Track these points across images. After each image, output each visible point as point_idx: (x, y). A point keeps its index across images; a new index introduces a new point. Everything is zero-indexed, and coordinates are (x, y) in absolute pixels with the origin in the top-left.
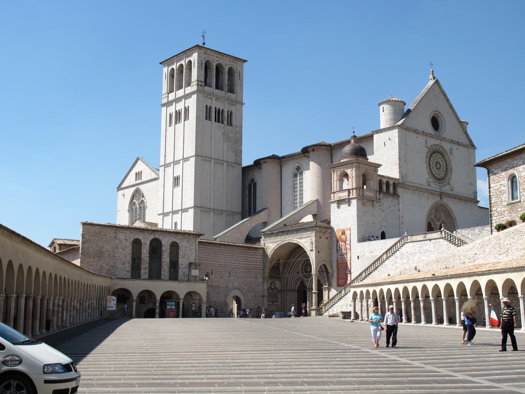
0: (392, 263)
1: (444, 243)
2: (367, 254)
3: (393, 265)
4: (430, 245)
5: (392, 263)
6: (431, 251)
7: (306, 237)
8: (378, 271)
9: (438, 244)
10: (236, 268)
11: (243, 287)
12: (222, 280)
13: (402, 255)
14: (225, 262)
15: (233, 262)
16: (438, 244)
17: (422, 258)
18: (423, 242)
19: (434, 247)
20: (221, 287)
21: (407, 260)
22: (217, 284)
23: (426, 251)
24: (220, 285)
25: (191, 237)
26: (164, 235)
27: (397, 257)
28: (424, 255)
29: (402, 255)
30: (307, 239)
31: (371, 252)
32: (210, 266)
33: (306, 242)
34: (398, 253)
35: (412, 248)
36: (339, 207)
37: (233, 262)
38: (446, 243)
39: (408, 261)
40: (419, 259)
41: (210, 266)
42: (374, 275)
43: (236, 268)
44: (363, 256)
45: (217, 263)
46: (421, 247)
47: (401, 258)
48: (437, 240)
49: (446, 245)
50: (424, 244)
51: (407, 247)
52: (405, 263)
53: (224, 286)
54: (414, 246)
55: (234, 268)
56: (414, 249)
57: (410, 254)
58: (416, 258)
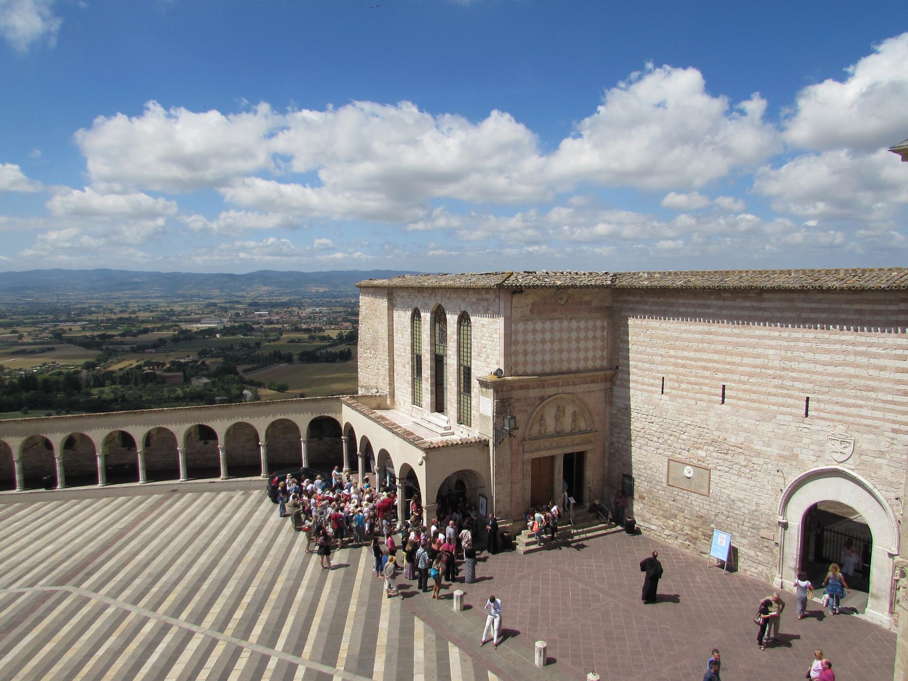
10: (843, 385)
11: (886, 472)
12: (766, 428)
14: (783, 359)
15: (826, 358)
20: (758, 454)
22: (741, 439)
24: (758, 446)
25: (491, 296)
26: (448, 295)
32: (717, 370)
37: (826, 358)
41: (717, 370)
43: (843, 385)
45: (746, 360)
53: (774, 450)
55: (834, 385)
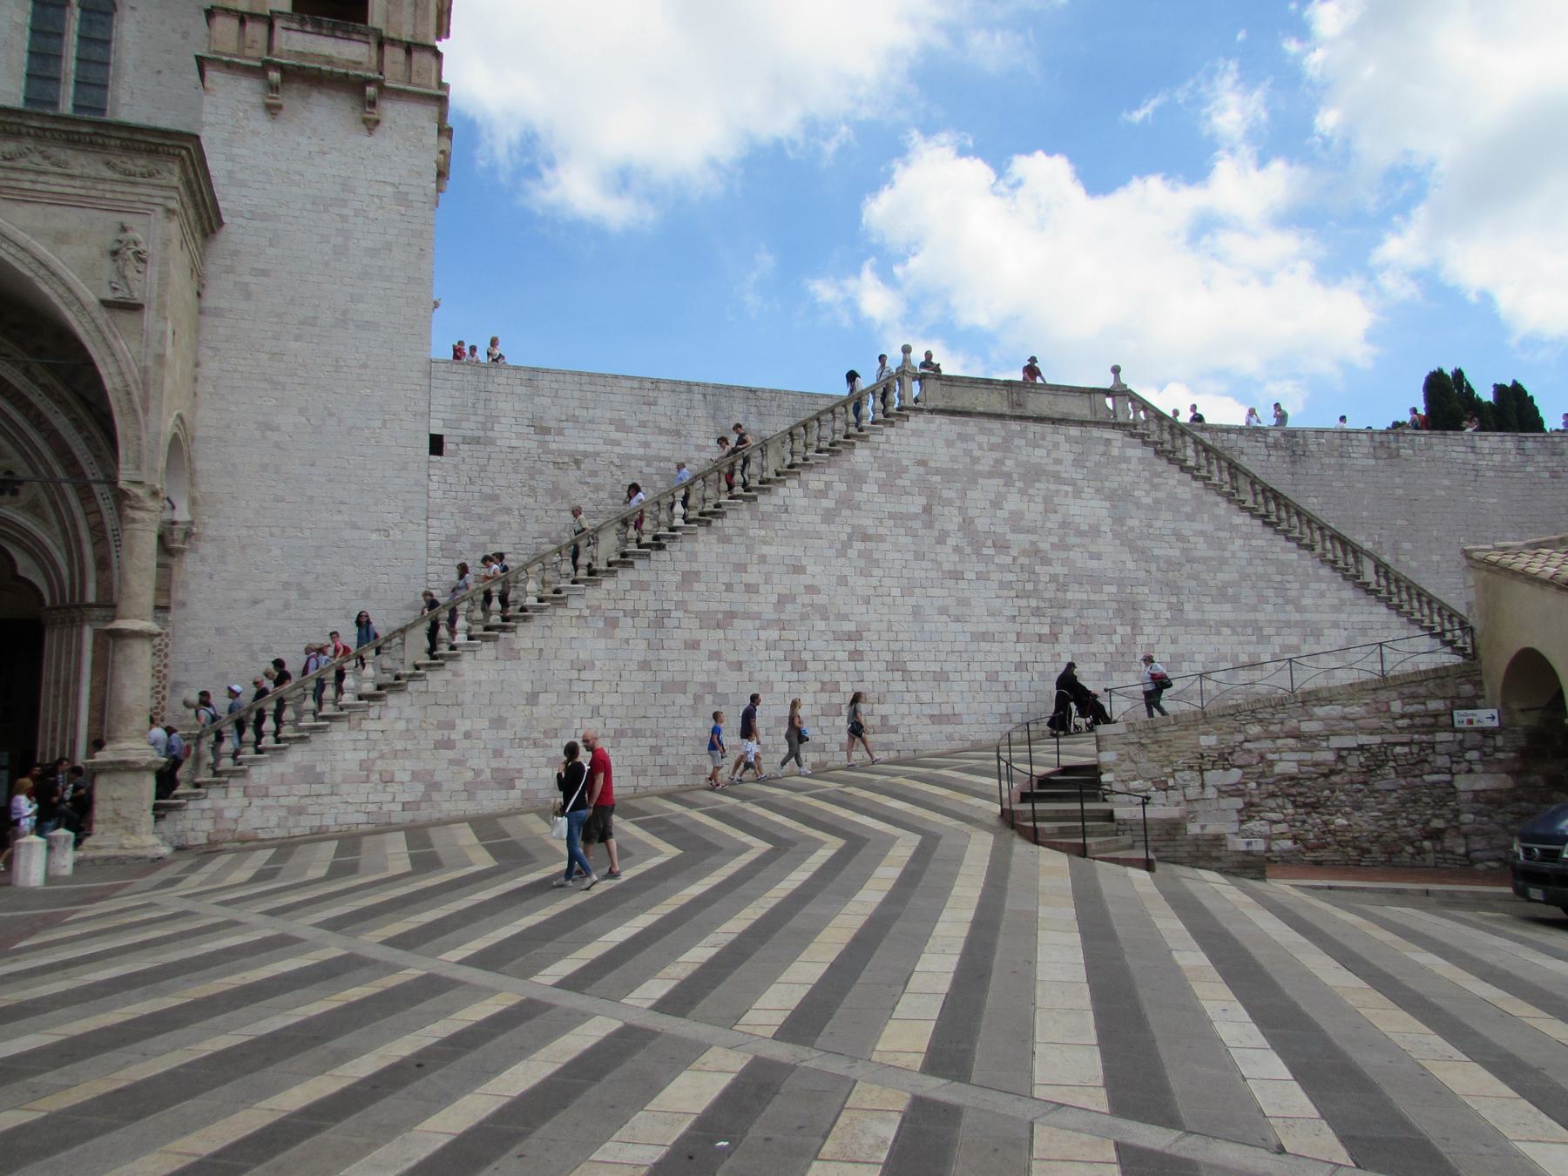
0: (828, 503)
1: (1130, 452)
2: (510, 434)
3: (829, 517)
4: (1056, 445)
5: (828, 503)
6: (1057, 478)
7: (60, 200)
8: (725, 539)
9: (1101, 449)
13: (894, 471)
16: (1101, 449)
17: (1013, 502)
18: (1015, 426)
19: (1078, 462)
21: (923, 500)
23: (1033, 474)
27: (857, 479)
28: (1022, 492)
29: (894, 471)
30: (70, 219)
31: (545, 431)
33: (61, 238)
34: (861, 455)
35: (949, 444)
36: (272, 109)
38: (1136, 452)
39: (927, 509)
40: (996, 504)
42: (693, 557)
44: (466, 441)
46: (1005, 446)
47: (886, 487)
48: (1096, 432)
49: (1141, 460)
50: (1023, 432)
51: (917, 433)
52: (915, 517)
54: (963, 437)
56: (968, 452)
57: (938, 472)
58: (978, 498)
